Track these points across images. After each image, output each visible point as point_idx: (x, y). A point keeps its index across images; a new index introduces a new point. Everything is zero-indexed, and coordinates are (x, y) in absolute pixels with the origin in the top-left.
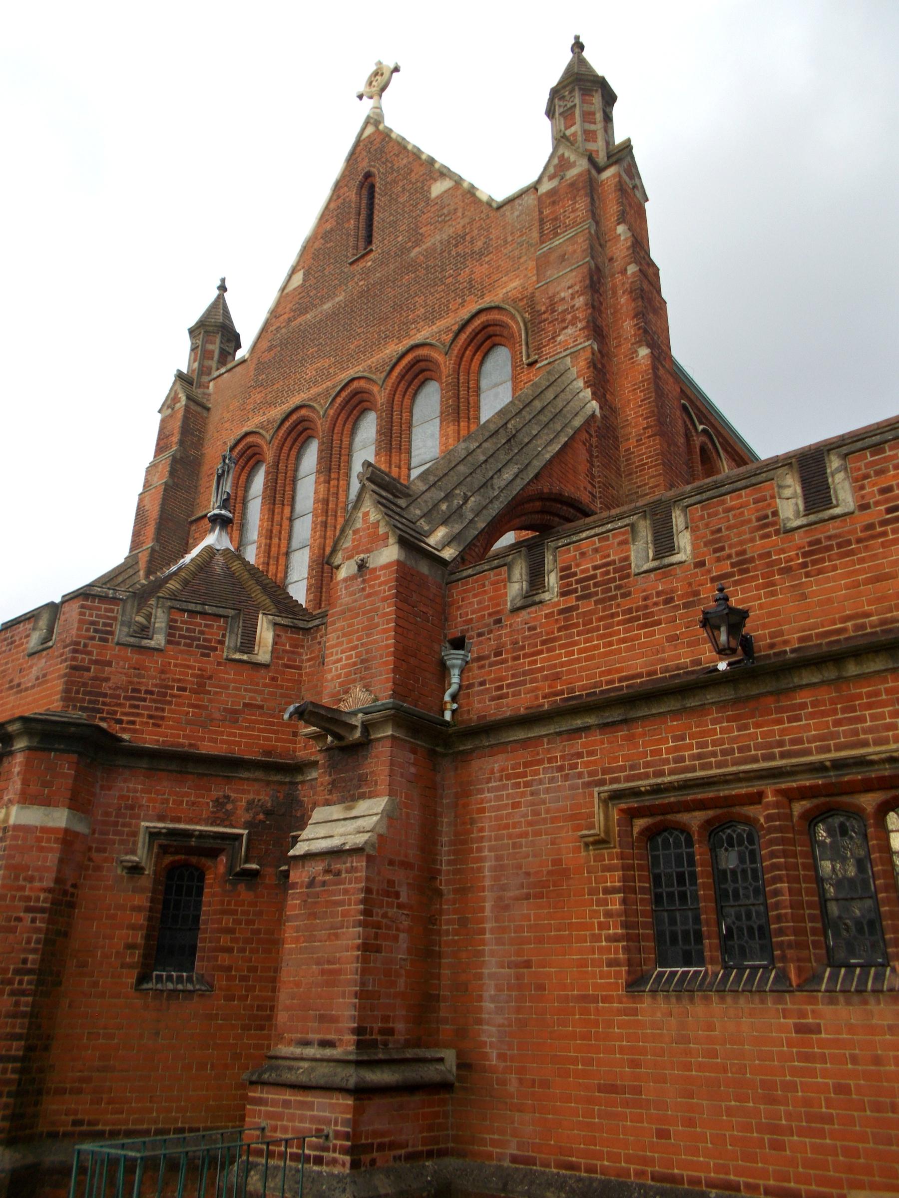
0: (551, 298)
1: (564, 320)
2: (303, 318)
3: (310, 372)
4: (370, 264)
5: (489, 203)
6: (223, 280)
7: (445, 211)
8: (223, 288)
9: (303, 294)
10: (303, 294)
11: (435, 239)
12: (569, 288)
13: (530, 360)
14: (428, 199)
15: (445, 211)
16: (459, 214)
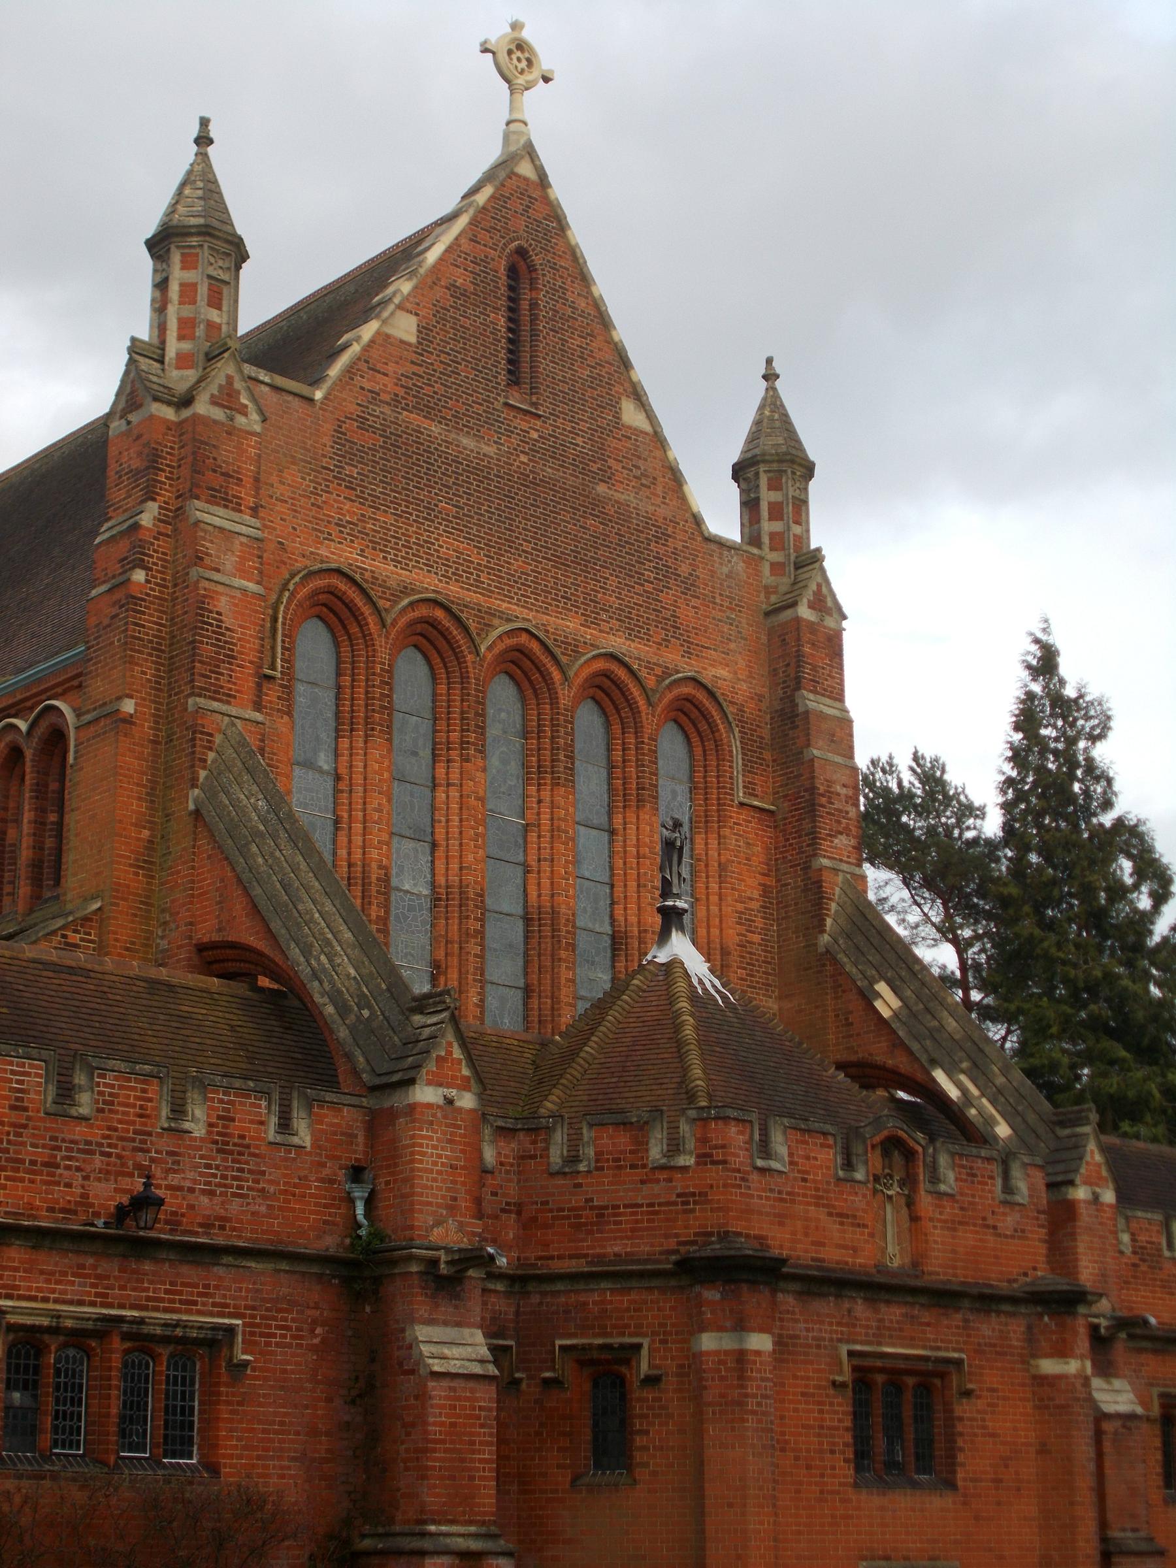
0: (830, 782)
1: (839, 822)
2: (426, 424)
3: (447, 545)
4: (535, 435)
5: (698, 521)
6: (204, 122)
7: (640, 463)
8: (203, 140)
9: (420, 371)
10: (420, 371)
11: (625, 496)
12: (844, 786)
13: (746, 801)
14: (617, 416)
15: (640, 463)
16: (659, 490)
